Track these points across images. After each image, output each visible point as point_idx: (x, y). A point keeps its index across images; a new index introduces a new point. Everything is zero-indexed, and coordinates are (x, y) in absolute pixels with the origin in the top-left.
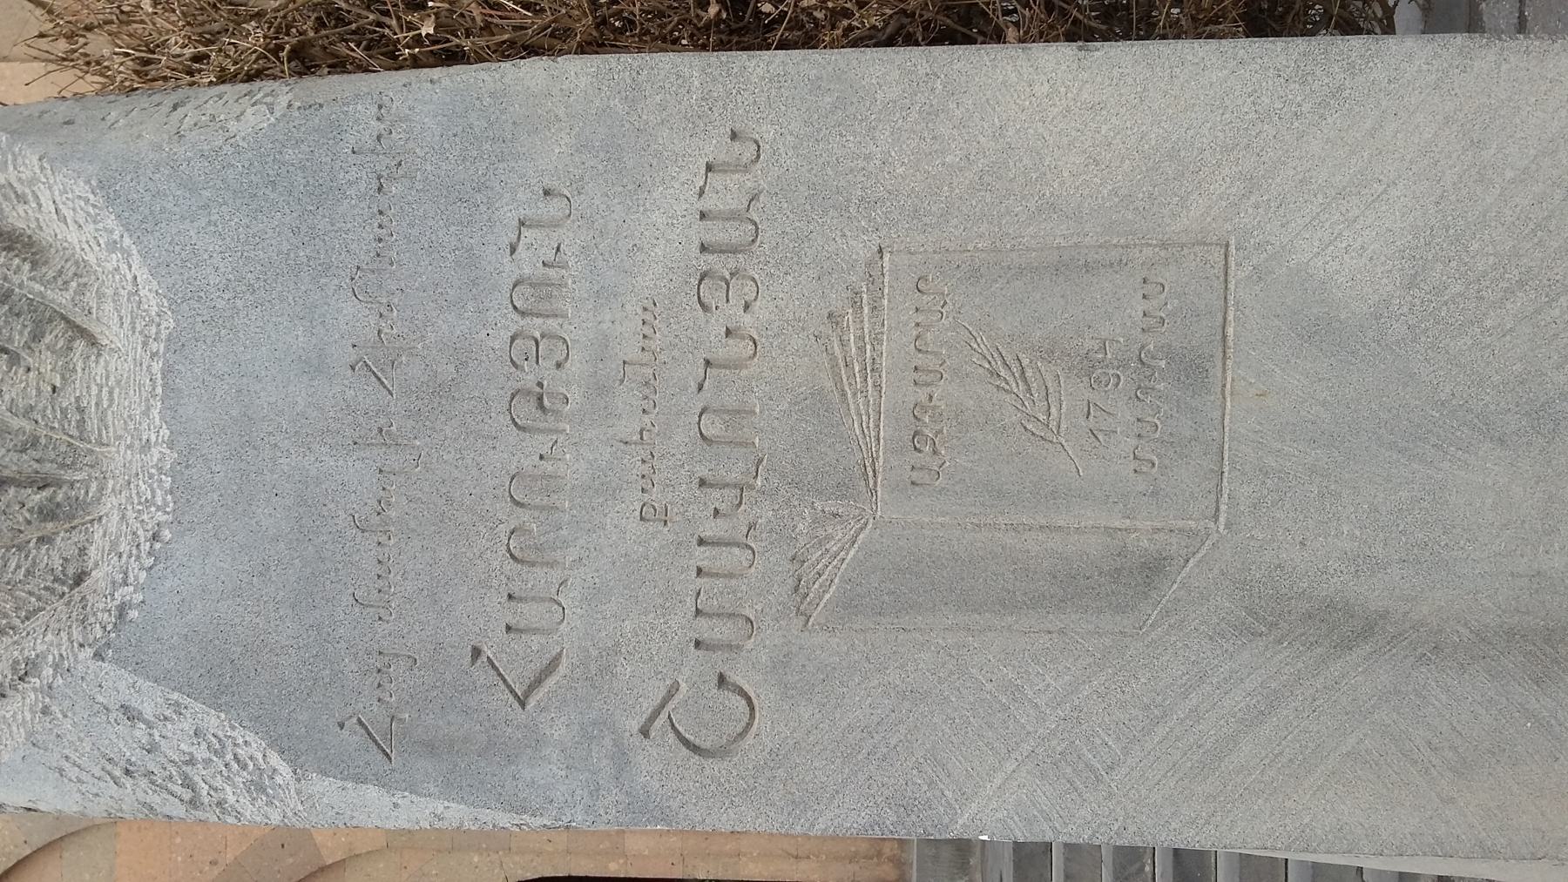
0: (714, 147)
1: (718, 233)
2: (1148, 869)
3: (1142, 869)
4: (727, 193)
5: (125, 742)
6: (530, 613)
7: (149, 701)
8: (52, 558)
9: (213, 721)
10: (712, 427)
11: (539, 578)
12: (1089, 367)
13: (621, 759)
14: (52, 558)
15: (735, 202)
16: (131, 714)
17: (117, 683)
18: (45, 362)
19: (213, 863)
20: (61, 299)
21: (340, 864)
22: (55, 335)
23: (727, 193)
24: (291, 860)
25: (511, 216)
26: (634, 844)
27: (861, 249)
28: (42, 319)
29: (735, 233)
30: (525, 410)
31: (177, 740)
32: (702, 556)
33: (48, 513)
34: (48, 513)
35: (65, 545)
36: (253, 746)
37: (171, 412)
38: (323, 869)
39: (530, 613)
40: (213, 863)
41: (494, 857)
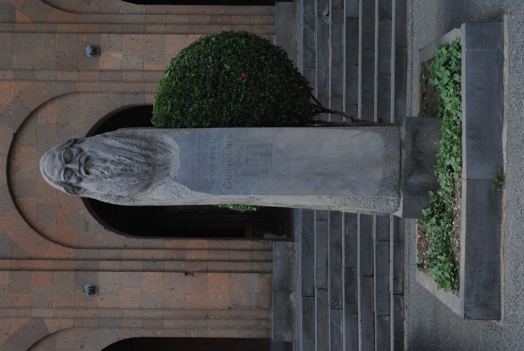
0: (229, 136)
1: (229, 143)
2: (340, 303)
3: (339, 303)
4: (230, 140)
5: (173, 190)
6: (213, 176)
7: (177, 184)
8: (166, 173)
9: (183, 186)
10: (229, 160)
11: (213, 173)
12: (261, 155)
13: (221, 189)
14: (166, 173)
15: (230, 140)
16: (175, 186)
17: (175, 183)
18: (165, 154)
19: (6, 334)
20: (168, 148)
21: (54, 333)
22: (166, 152)
23: (230, 140)
24: (36, 332)
25: (211, 141)
26: (167, 323)
27: (241, 144)
28: (165, 150)
29: (231, 143)
30: (212, 159)
31: (179, 189)
32: (228, 171)
33: (165, 168)
34: (165, 168)
35: (167, 171)
36: (187, 189)
37: (180, 159)
38: (49, 336)
39: (213, 176)
40: (6, 334)
41: (114, 330)
